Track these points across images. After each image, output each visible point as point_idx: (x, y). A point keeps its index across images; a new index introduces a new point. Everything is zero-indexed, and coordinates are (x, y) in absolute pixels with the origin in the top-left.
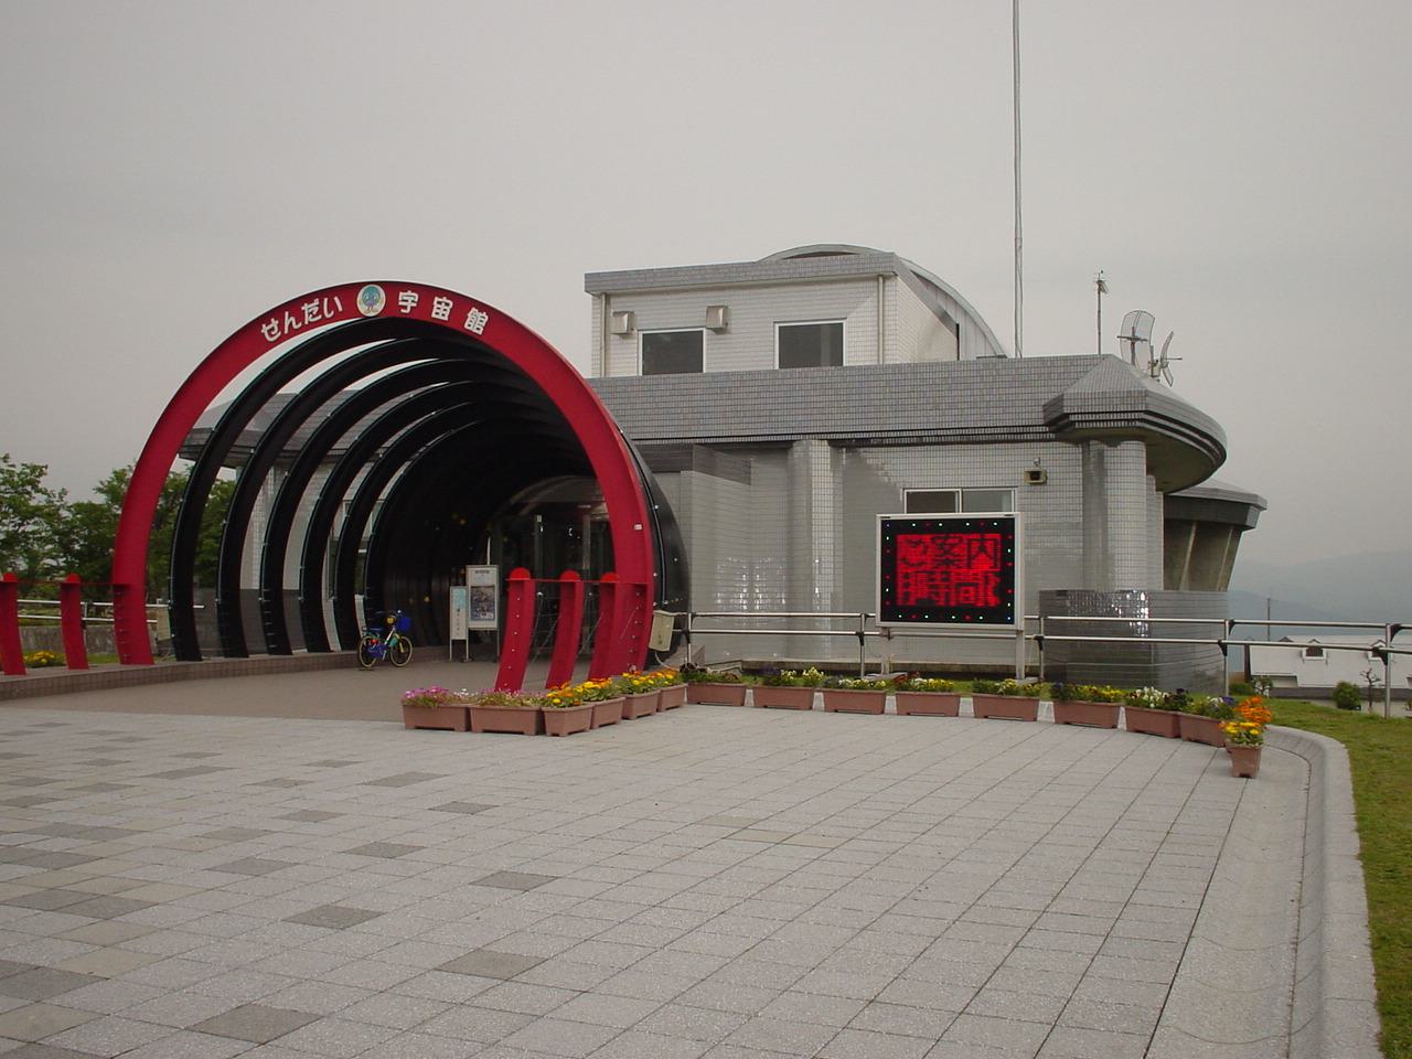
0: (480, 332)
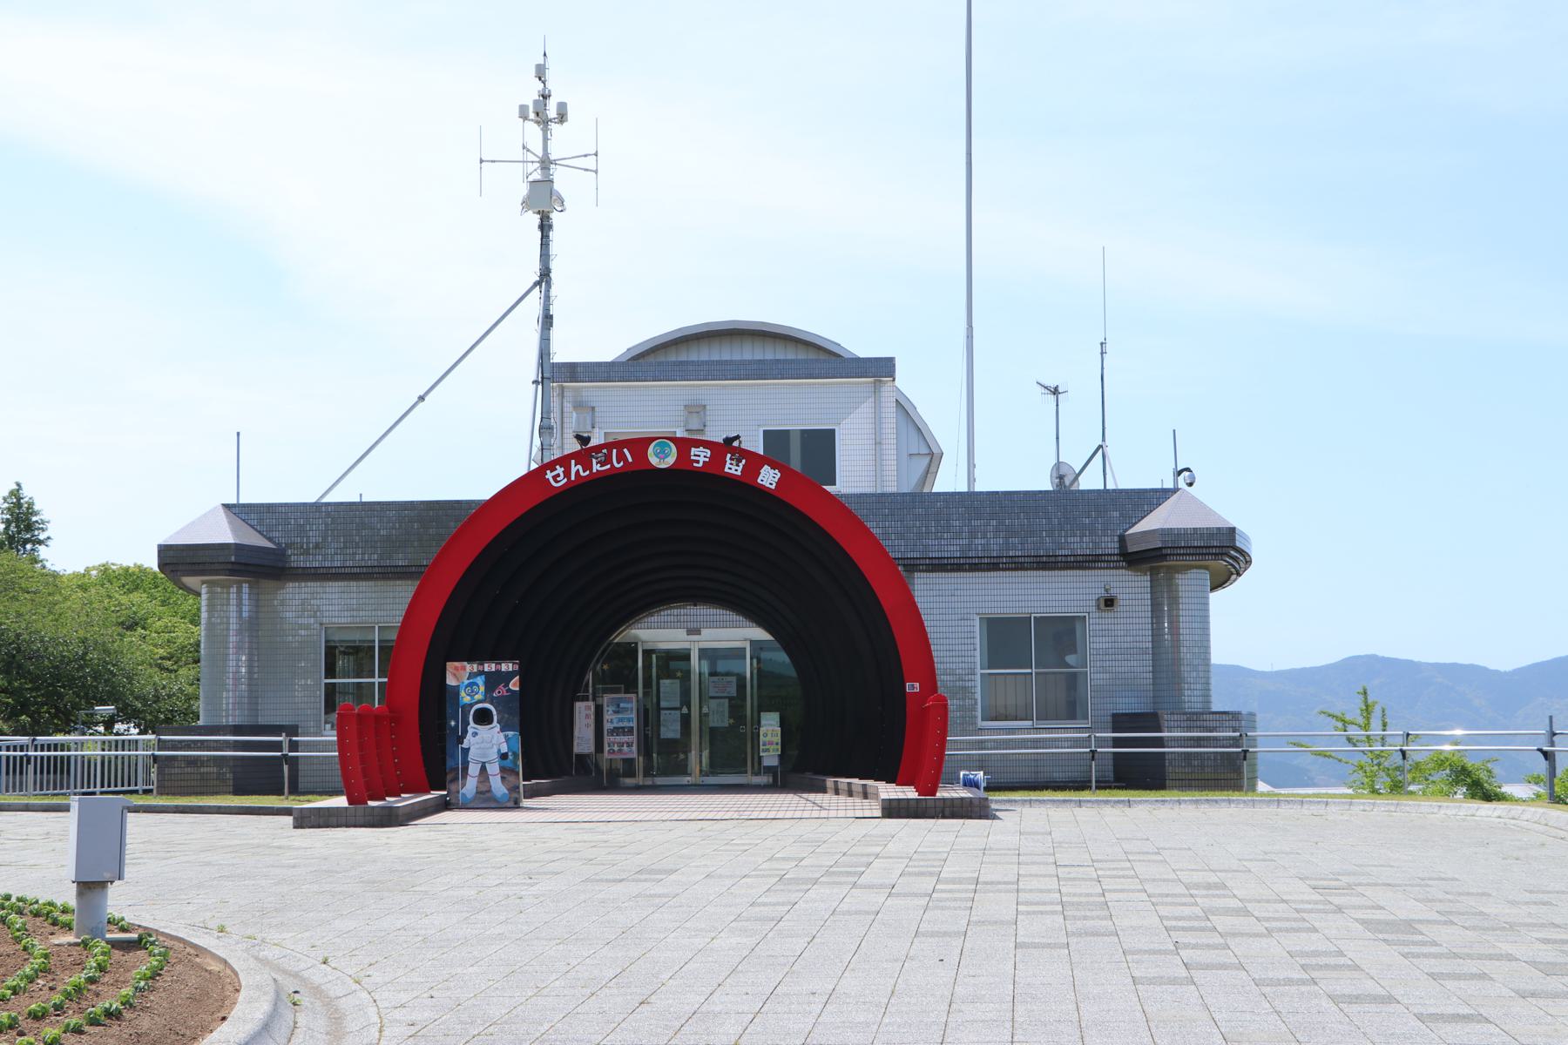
0: (773, 487)
